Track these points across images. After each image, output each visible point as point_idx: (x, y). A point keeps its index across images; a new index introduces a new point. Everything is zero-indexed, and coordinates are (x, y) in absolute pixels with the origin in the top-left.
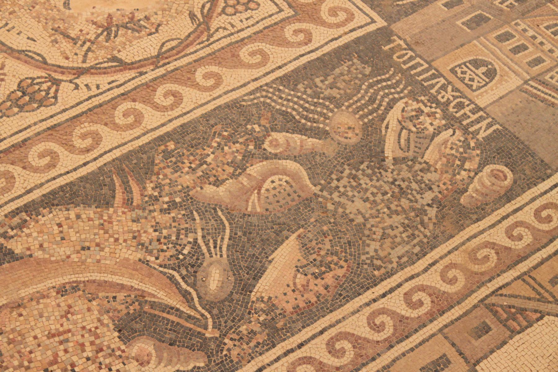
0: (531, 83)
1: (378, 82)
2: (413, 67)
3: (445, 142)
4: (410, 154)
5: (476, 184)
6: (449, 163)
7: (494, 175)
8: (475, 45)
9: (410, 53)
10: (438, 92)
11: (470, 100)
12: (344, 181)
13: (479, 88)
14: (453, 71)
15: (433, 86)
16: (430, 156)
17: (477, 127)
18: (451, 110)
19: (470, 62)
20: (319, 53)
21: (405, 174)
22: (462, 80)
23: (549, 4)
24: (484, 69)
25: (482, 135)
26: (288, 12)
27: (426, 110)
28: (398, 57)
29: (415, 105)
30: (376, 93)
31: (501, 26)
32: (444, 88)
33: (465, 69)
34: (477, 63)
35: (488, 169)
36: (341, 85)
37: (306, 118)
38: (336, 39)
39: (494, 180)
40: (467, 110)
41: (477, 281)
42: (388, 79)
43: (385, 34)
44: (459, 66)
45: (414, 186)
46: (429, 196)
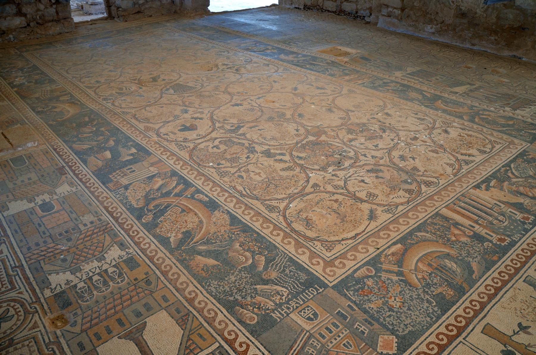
0: (308, 333)
1: (296, 284)
2: (307, 294)
3: (268, 303)
4: (259, 292)
5: (246, 312)
6: (255, 303)
7: (252, 319)
8: (326, 315)
9: (315, 293)
10: (294, 301)
11: (292, 311)
12: (244, 275)
13: (301, 315)
14: (308, 306)
15: (298, 300)
16: (259, 298)
17: (277, 313)
18: (285, 305)
19: (315, 312)
20: (308, 268)
21: (249, 291)
22: (304, 309)
23: (364, 344)
24: (312, 317)
25: (273, 315)
26: (328, 260)
27: (284, 298)
28: (312, 290)
29: (285, 294)
30: (289, 283)
31: (342, 324)
32: (297, 303)
33: (310, 311)
34: (316, 315)
35: (254, 316)
36: (292, 273)
37: (273, 265)
38: (317, 272)
39: (249, 318)
40: (286, 310)
41: (200, 311)
42: (298, 286)
43: (325, 286)
44: (312, 308)
45: (244, 294)
46: (239, 298)
